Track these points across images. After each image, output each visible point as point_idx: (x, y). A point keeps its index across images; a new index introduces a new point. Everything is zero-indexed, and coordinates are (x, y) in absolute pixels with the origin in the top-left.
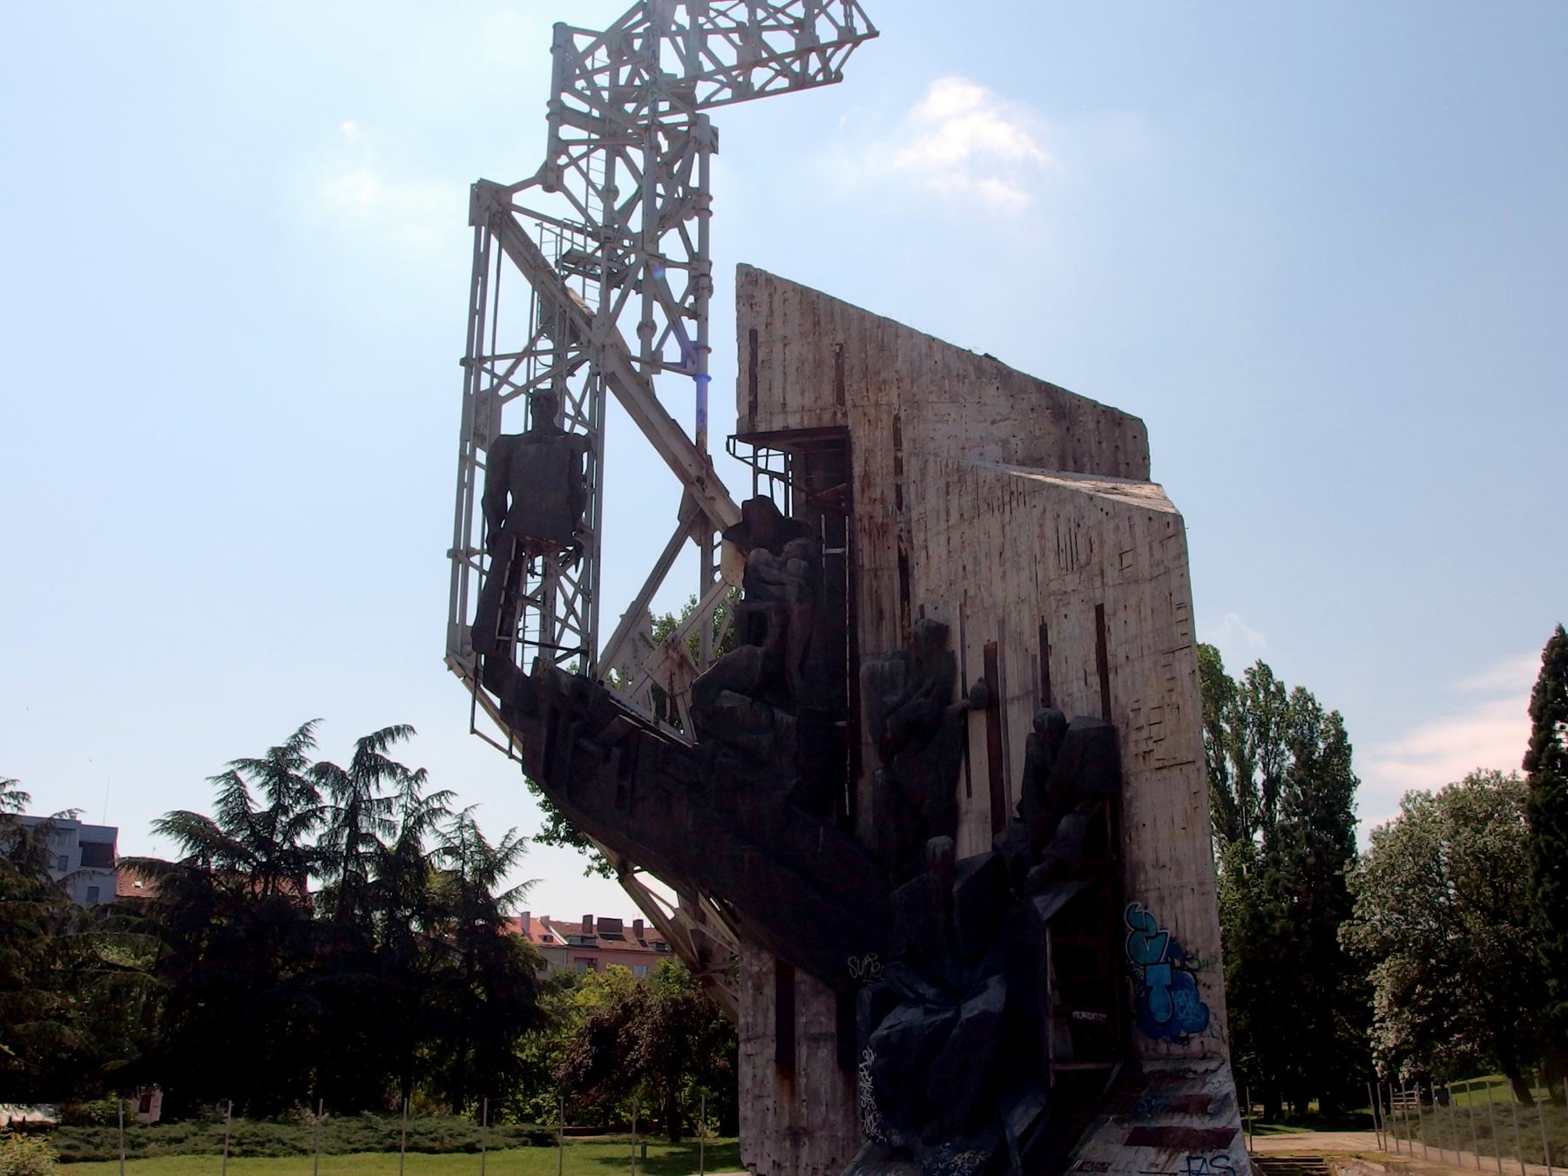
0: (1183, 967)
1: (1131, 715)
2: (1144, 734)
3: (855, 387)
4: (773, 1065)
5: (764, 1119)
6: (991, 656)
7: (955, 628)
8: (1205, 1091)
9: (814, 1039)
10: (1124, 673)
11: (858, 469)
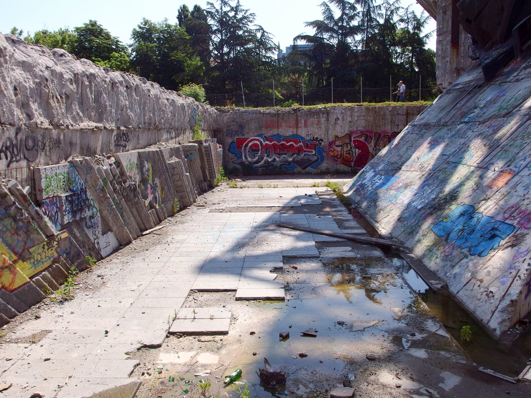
4: (450, 43)
5: (446, 66)
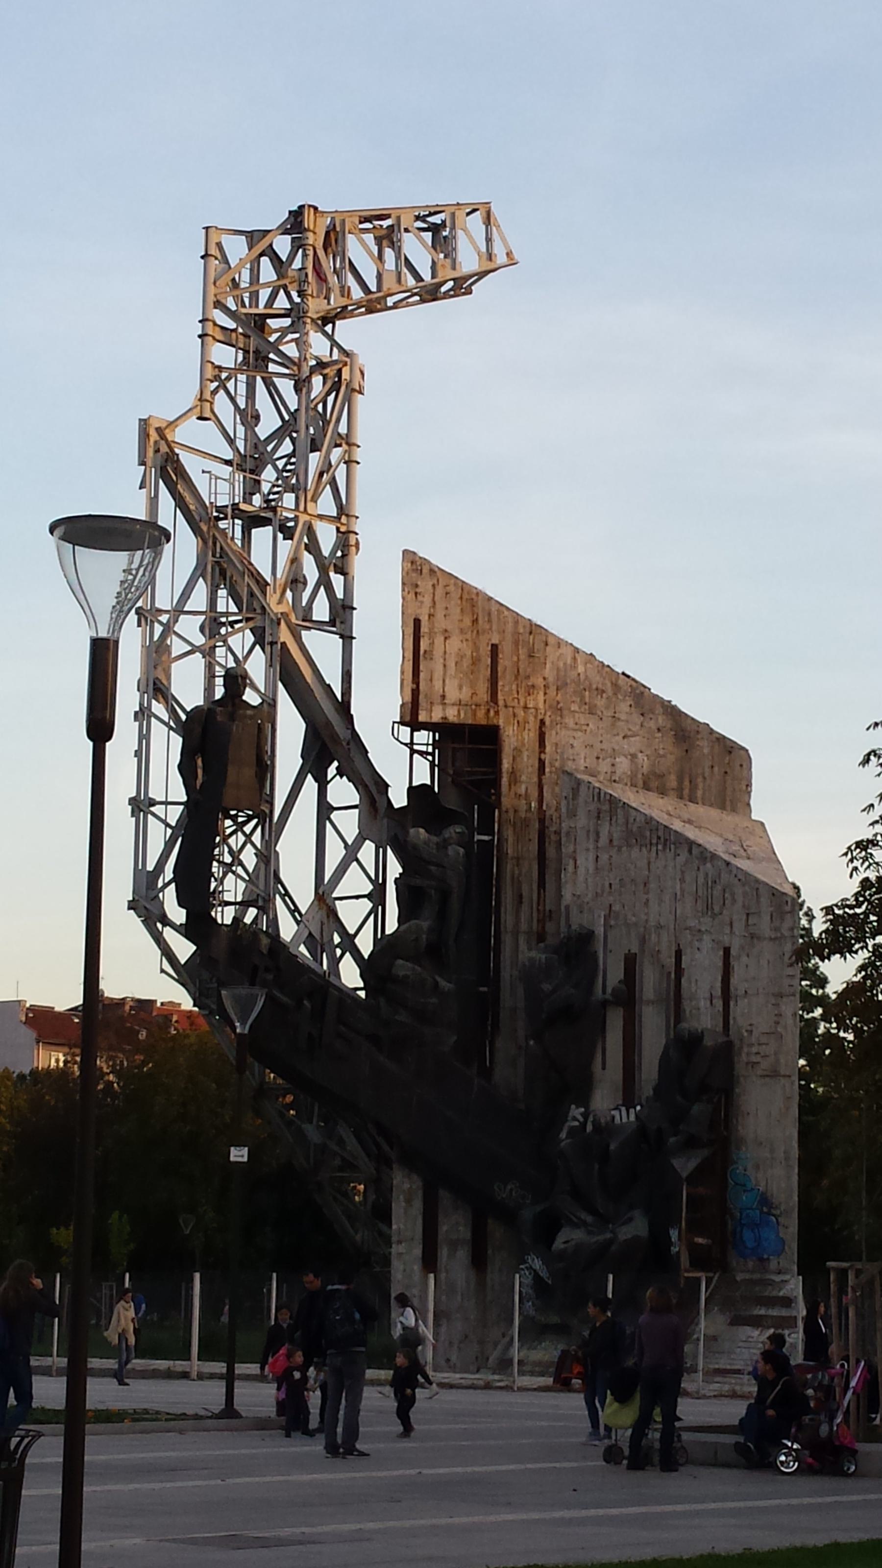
0: (769, 1214)
1: (745, 1034)
2: (754, 1050)
3: (506, 689)
6: (631, 963)
7: (600, 931)
8: (781, 1294)
9: (454, 1245)
10: (743, 1003)
11: (506, 765)
